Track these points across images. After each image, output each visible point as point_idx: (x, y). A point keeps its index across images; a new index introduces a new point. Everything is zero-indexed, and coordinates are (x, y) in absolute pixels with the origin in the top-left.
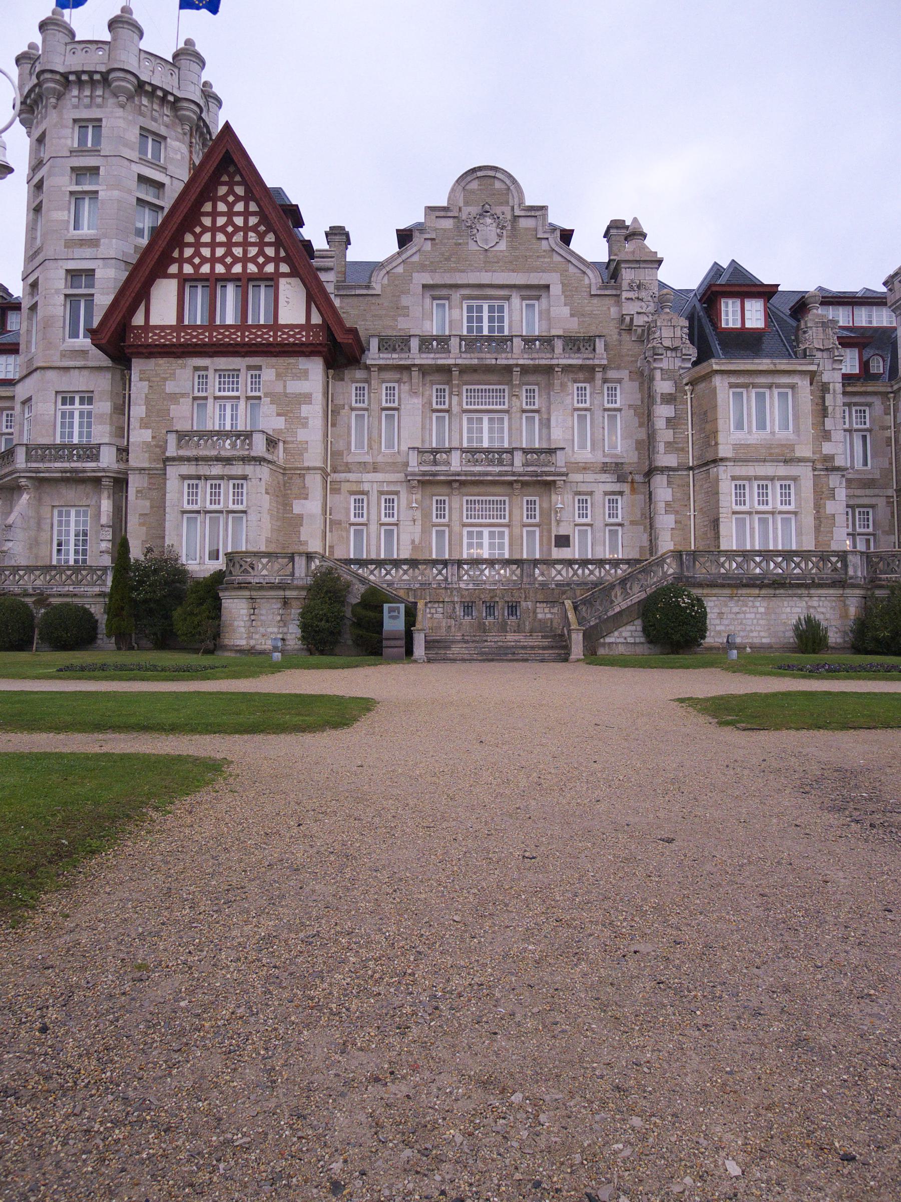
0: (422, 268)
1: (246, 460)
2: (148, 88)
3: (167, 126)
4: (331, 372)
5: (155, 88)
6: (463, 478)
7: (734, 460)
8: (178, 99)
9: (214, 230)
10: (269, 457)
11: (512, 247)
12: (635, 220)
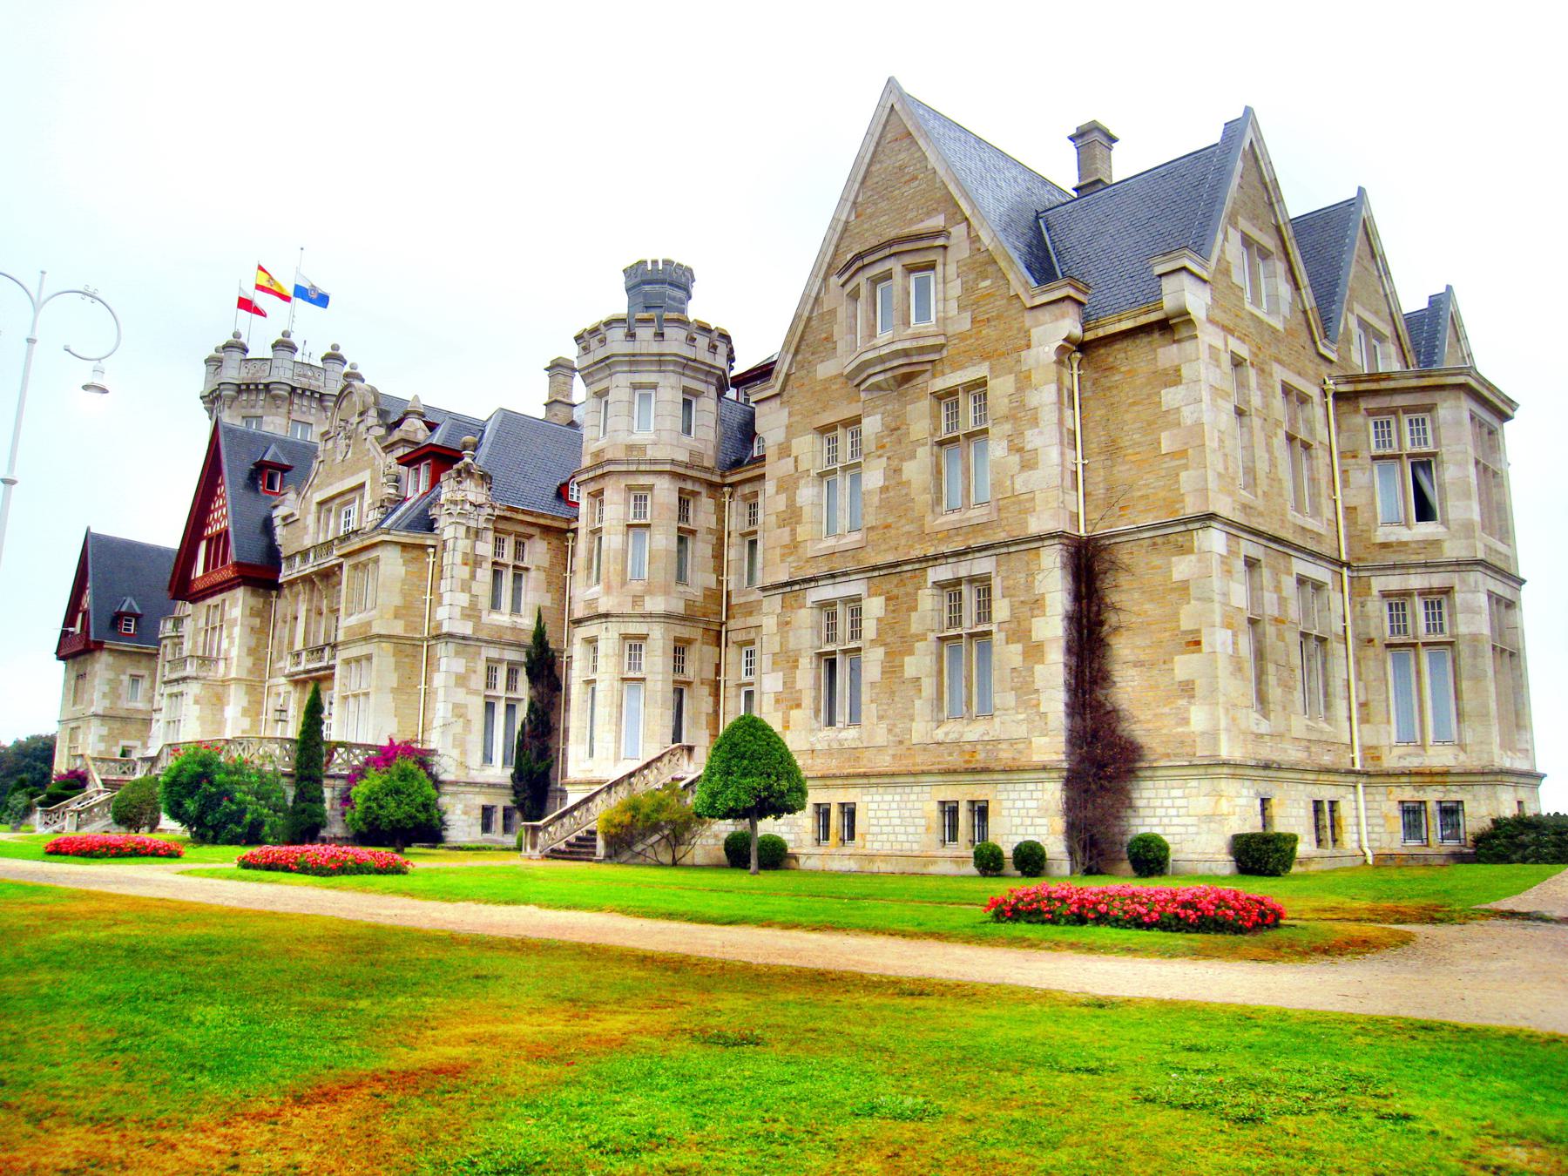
0: (319, 488)
1: (184, 679)
2: (243, 387)
3: (263, 407)
4: (274, 593)
5: (248, 385)
6: (303, 676)
7: (344, 643)
8: (267, 386)
9: (219, 497)
10: (202, 674)
11: (353, 453)
12: (416, 397)
